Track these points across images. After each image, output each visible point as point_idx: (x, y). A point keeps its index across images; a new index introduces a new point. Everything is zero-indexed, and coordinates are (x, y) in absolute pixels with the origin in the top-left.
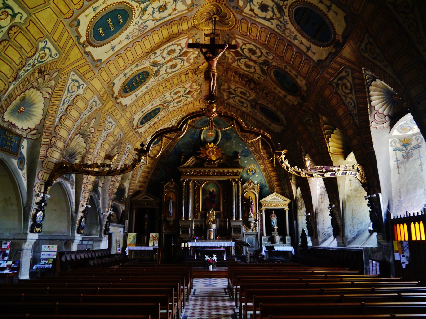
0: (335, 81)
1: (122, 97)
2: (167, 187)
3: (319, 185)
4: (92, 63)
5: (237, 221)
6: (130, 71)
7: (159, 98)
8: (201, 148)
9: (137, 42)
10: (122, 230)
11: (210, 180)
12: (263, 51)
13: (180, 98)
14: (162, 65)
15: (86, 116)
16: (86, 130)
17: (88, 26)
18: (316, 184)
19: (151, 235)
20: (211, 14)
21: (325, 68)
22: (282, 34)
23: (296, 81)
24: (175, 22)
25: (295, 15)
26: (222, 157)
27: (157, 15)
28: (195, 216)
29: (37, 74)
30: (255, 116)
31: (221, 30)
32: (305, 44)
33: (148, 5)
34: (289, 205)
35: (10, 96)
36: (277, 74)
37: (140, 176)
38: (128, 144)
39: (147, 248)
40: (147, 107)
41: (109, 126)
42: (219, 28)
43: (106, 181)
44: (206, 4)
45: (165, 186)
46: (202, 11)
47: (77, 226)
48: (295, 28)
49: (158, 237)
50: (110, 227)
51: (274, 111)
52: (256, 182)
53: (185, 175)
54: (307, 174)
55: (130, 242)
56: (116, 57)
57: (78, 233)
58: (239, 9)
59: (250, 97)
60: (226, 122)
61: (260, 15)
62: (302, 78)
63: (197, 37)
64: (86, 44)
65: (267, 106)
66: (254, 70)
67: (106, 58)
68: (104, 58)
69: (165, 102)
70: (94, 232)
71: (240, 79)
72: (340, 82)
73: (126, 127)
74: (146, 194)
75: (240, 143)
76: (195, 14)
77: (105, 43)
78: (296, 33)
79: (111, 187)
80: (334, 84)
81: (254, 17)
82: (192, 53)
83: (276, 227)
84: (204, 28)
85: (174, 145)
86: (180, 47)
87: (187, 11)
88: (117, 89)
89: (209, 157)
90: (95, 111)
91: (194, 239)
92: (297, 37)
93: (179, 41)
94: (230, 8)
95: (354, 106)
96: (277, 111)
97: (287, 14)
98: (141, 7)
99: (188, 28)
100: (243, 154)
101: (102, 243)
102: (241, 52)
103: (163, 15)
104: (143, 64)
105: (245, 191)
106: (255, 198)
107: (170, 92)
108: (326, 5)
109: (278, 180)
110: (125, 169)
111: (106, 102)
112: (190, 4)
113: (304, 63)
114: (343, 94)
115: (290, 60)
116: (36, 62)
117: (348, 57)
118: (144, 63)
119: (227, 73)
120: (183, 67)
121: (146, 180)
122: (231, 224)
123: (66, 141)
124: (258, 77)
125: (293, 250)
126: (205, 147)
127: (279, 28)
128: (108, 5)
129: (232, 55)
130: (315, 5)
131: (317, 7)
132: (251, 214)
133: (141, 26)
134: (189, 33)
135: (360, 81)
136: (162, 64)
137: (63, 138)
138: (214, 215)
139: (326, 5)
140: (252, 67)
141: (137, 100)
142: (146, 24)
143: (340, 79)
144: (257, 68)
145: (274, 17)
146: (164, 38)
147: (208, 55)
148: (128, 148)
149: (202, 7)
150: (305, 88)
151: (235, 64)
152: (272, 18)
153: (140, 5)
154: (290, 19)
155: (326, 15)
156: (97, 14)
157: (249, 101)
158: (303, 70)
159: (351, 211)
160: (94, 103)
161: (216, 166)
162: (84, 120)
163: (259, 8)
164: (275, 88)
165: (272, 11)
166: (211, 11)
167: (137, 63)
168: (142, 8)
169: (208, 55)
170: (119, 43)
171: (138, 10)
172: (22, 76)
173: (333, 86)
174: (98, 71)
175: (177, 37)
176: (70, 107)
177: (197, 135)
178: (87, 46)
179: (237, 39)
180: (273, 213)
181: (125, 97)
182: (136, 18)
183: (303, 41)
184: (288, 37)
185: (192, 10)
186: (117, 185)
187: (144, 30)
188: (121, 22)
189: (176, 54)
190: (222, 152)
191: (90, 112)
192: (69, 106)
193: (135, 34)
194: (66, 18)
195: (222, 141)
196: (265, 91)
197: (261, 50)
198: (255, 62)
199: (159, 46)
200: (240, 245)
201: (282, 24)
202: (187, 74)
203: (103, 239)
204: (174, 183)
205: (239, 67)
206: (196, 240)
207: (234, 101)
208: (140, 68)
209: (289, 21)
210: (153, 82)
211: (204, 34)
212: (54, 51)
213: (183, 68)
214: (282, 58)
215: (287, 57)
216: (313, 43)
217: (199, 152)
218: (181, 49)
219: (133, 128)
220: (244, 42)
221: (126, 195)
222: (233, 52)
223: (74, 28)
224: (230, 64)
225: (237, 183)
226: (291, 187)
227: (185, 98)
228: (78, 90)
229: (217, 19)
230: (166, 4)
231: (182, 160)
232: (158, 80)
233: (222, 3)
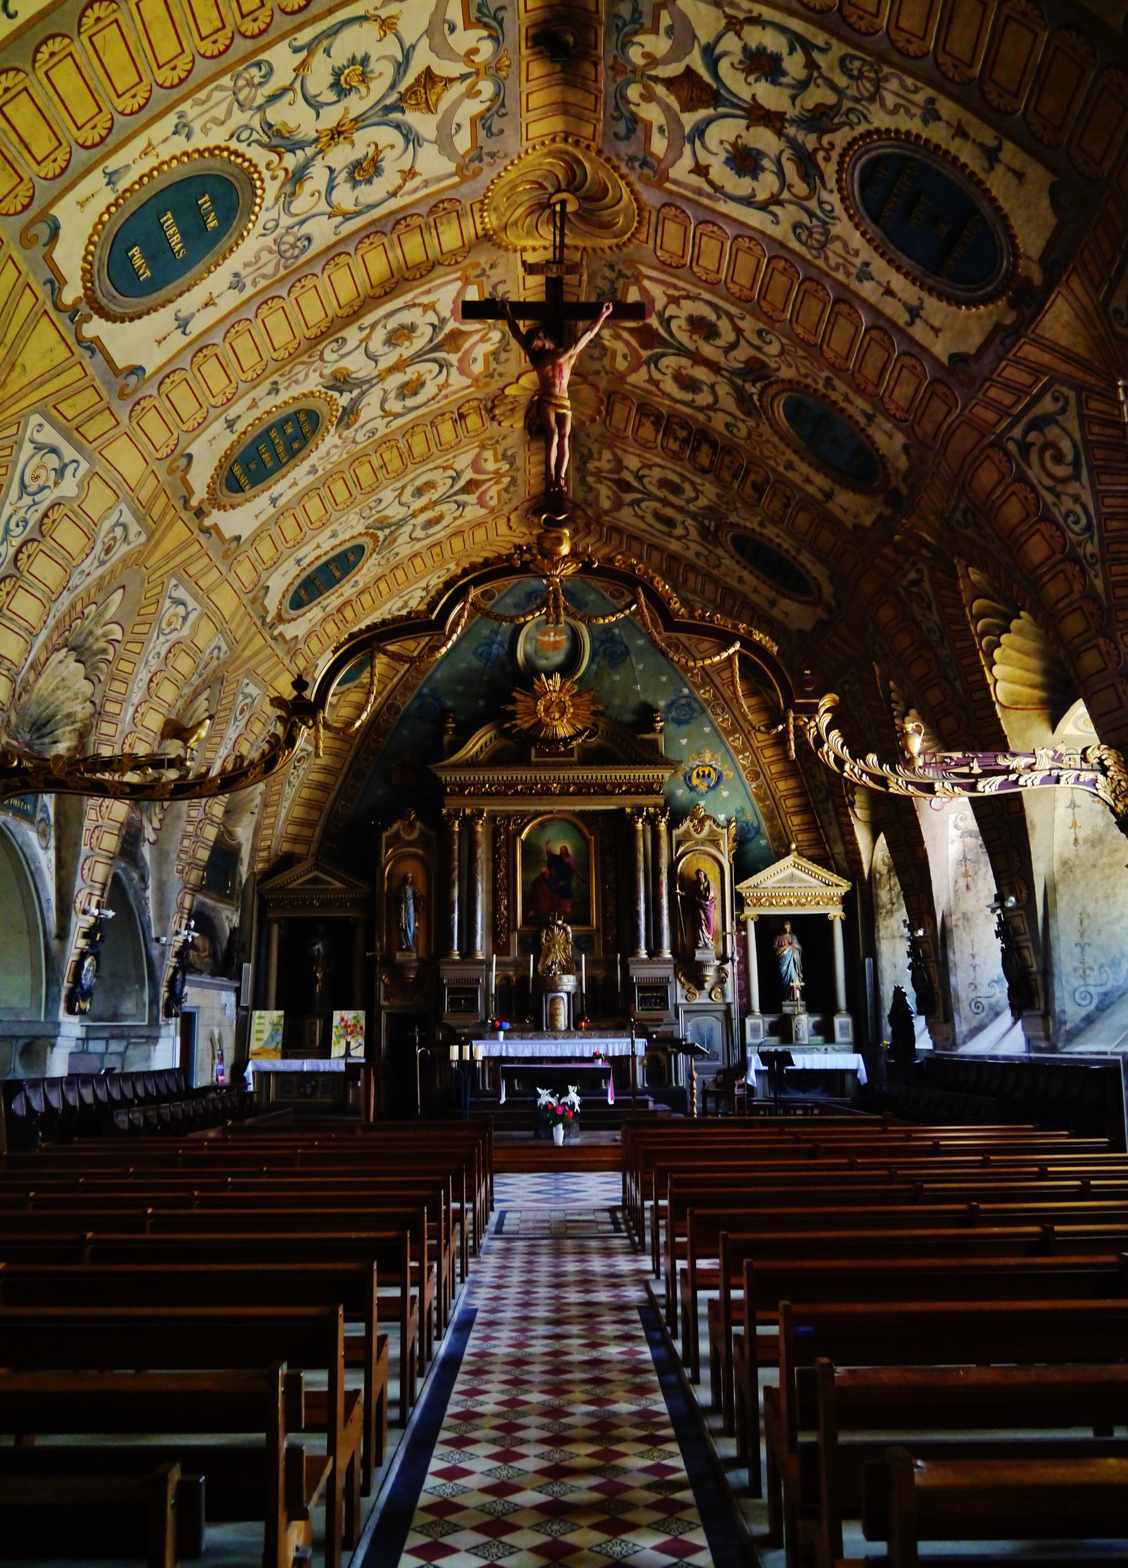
0: (1017, 433)
1: (223, 508)
2: (395, 840)
3: (956, 827)
4: (107, 383)
5: (655, 963)
6: (249, 409)
7: (357, 510)
8: (515, 694)
9: (273, 298)
10: (232, 998)
11: (551, 812)
12: (741, 324)
13: (437, 508)
14: (366, 384)
15: (89, 579)
16: (91, 633)
17: (90, 242)
18: (945, 823)
19: (337, 1015)
20: (545, 188)
22: (816, 258)
23: (869, 437)
24: (415, 221)
25: (862, 187)
26: (594, 724)
27: (345, 197)
28: (498, 947)
30: (715, 572)
31: (585, 249)
32: (899, 295)
33: (313, 158)
34: (847, 901)
36: (795, 411)
37: (293, 800)
38: (246, 681)
39: (323, 1065)
40: (313, 544)
41: (176, 615)
42: (580, 243)
43: (168, 821)
44: (527, 152)
45: (385, 835)
46: (512, 176)
47: (66, 986)
48: (863, 234)
49: (363, 1022)
50: (186, 989)
51: (787, 551)
52: (722, 818)
53: (461, 793)
54: (913, 784)
55: (261, 1044)
56: (195, 356)
57: (70, 1010)
58: (651, 167)
59: (697, 498)
60: (607, 595)
61: (730, 188)
63: (496, 275)
64: (85, 309)
65: (762, 534)
66: (710, 399)
67: (160, 360)
68: (152, 360)
69: (382, 523)
70: (128, 1007)
71: (657, 431)
72: (1032, 436)
73: (238, 618)
74: (317, 867)
75: (662, 674)
76: (489, 190)
77: (152, 304)
78: (866, 253)
79: (186, 843)
80: (1011, 446)
81: (709, 197)
82: (477, 337)
83: (797, 983)
84: (521, 243)
85: (415, 686)
86: (431, 317)
87: (456, 179)
88: (201, 478)
89: (547, 725)
90: (124, 559)
91: (495, 1030)
92: (872, 268)
93: (429, 291)
94: (616, 162)
95: (1089, 527)
96: (798, 551)
97: (832, 183)
98: (284, 164)
99: (460, 244)
100: (674, 714)
101: (158, 1047)
102: (661, 331)
103: (369, 193)
104: (297, 382)
105: (681, 850)
106: (718, 876)
107: (399, 485)
108: (982, 147)
109: (804, 809)
110: (240, 775)
111: (163, 527)
112: (467, 152)
113: (898, 366)
114: (1047, 482)
115: (847, 358)
117: (1063, 343)
118: (301, 377)
119: (609, 413)
120: (444, 392)
121: (315, 815)
122: (632, 972)
123: (18, 674)
124: (727, 425)
125: (862, 1067)
126: (533, 691)
127: (804, 237)
128: (163, 163)
129: (627, 343)
130: (937, 147)
131: (947, 152)
132: (706, 936)
133: (286, 239)
134: (467, 262)
135: (1108, 431)
136: (368, 381)
137: (8, 663)
138: (567, 942)
139: (982, 147)
140: (705, 388)
141: (276, 519)
142: (306, 229)
143: (1031, 427)
144: (723, 390)
145: (786, 195)
146: (374, 283)
147: (537, 343)
148: (246, 696)
149: (512, 163)
150: (903, 463)
151: (639, 378)
152: (775, 200)
154: (843, 200)
155: (980, 182)
156: (122, 196)
157: (694, 516)
158: (896, 394)
159: (1077, 921)
160: (119, 531)
161: (575, 759)
162: (84, 595)
163: (727, 162)
164: (790, 466)
166: (545, 178)
168: (290, 170)
169: (537, 343)
170: (206, 305)
171: (274, 178)
173: (1006, 453)
174: (132, 411)
175: (422, 276)
176: (31, 548)
177: (501, 644)
178: (88, 319)
179: (647, 283)
180: (785, 932)
181: (233, 507)
182: (267, 210)
183: (893, 285)
184: (836, 268)
185: (477, 174)
186: (211, 833)
187: (297, 251)
188: (212, 223)
189: (420, 341)
190: (593, 708)
191: (102, 563)
192: (25, 543)
193: (263, 271)
194: (7, 214)
195: (594, 667)
196: (752, 477)
197: (737, 321)
198: (713, 367)
199: (353, 315)
200: (664, 1050)
201: (815, 222)
202: (462, 417)
203: (164, 1032)
204: (418, 825)
205: (654, 389)
206: (501, 1034)
207: (636, 515)
208: (284, 396)
210: (333, 451)
211: (524, 263)
213: (446, 397)
214: (814, 350)
215: (832, 345)
216: (930, 291)
217: (511, 708)
218: (436, 322)
219: (264, 623)
220: (670, 292)
221: (244, 870)
222: (630, 330)
223: (39, 251)
224: (622, 377)
225: (652, 820)
226: (853, 833)
227: (455, 506)
228: (56, 484)
229: (570, 208)
230: (378, 152)
231: (446, 738)
232: (354, 441)
233: (588, 147)
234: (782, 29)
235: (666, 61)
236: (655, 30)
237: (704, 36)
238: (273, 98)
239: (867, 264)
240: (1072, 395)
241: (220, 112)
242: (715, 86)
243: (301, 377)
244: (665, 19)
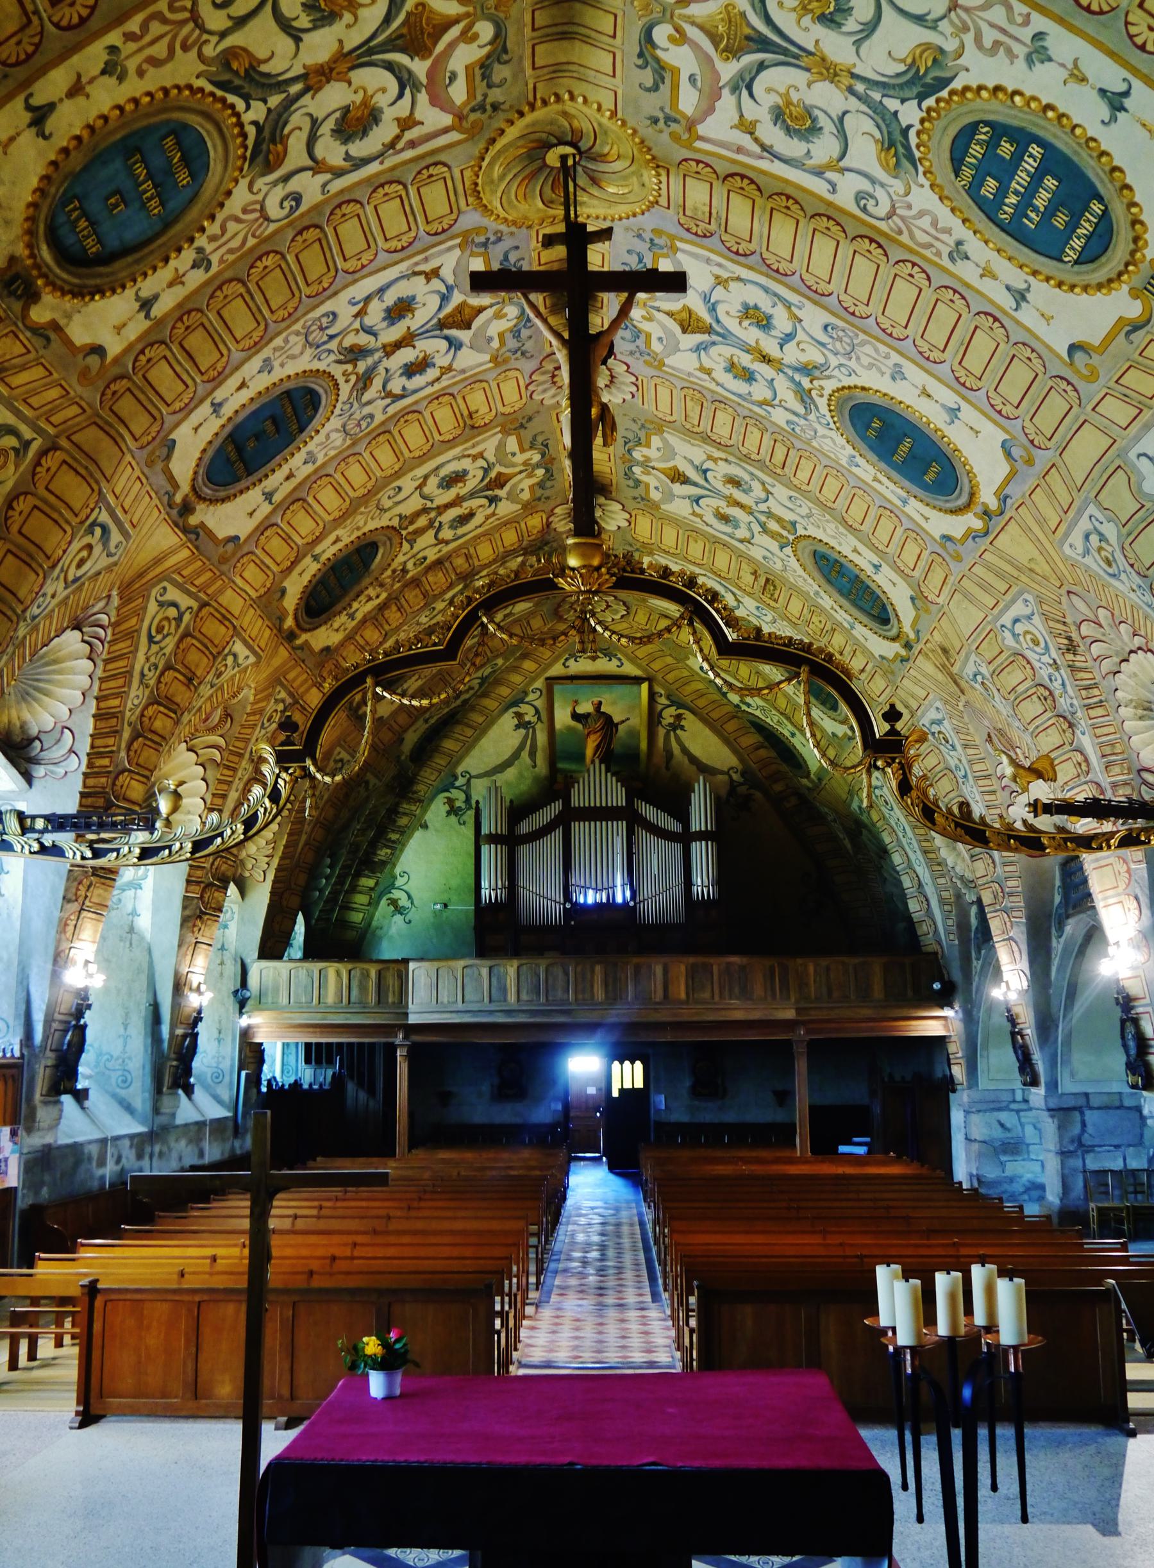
0: (104, 517)
6: (994, 277)
21: (146, 470)
29: (1078, 658)
35: (1108, 750)
61: (403, 283)
62: (133, 338)
81: (417, 264)
93: (740, 150)
94: (513, 229)
104: (934, 224)
113: (189, 382)
127: (324, 320)
150: (80, 335)
167: (946, 262)
172: (1072, 705)
179: (447, 120)
183: (244, 391)
184: (286, 341)
197: (328, 176)
201: (325, 338)
212: (1018, 609)
234: (415, 391)
236: (501, 336)
238: (795, 414)
241: (828, 441)
242: (446, 332)
243: (925, 222)
244: (495, 344)
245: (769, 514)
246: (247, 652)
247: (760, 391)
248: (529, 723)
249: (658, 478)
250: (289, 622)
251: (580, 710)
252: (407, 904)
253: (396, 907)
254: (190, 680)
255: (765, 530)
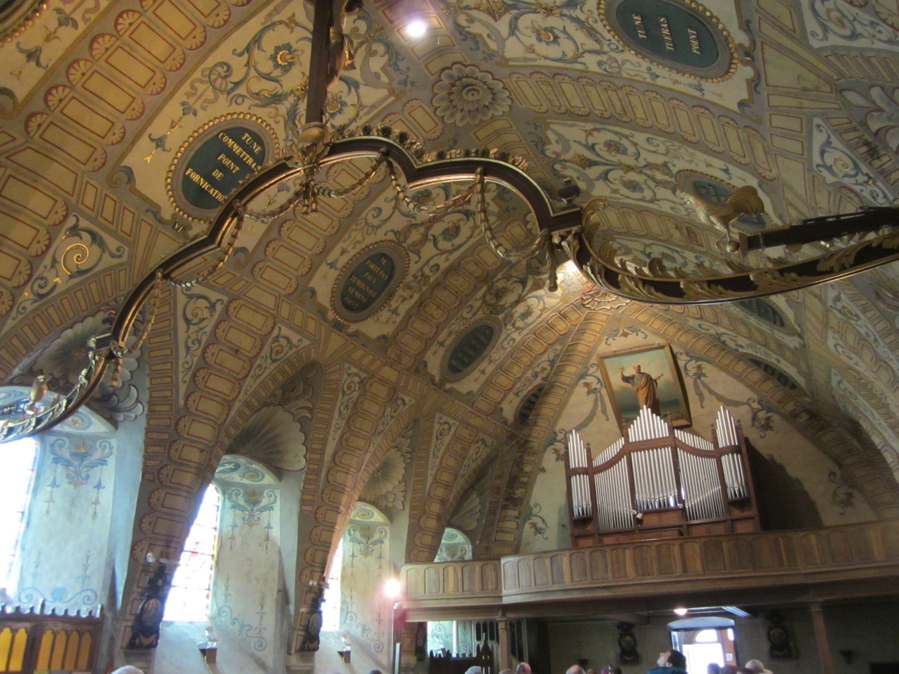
0: (83, 223)
22: (203, 71)
78: (204, 116)
80: (71, 221)
81: (270, 15)
95: (41, 296)
116: (861, 178)
127: (219, 69)
153: (587, 19)
165: (269, 74)
173: (65, 217)
184: (193, 87)
201: (231, 86)
209: (234, 108)
235: (366, 62)
237: (363, 89)
239: (195, 114)
240: (125, 259)
244: (384, 79)
245: (648, 165)
246: (299, 337)
247: (566, 46)
248: (596, 389)
249: (573, 169)
250: (331, 315)
251: (627, 374)
252: (543, 526)
253: (536, 529)
254: (237, 351)
255: (658, 183)
